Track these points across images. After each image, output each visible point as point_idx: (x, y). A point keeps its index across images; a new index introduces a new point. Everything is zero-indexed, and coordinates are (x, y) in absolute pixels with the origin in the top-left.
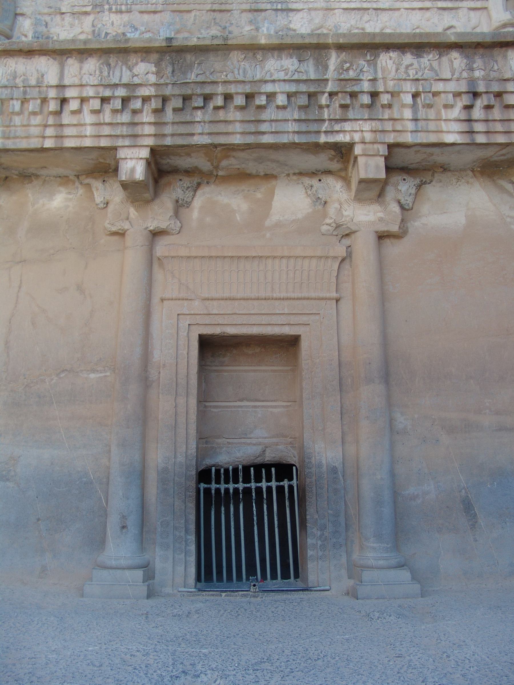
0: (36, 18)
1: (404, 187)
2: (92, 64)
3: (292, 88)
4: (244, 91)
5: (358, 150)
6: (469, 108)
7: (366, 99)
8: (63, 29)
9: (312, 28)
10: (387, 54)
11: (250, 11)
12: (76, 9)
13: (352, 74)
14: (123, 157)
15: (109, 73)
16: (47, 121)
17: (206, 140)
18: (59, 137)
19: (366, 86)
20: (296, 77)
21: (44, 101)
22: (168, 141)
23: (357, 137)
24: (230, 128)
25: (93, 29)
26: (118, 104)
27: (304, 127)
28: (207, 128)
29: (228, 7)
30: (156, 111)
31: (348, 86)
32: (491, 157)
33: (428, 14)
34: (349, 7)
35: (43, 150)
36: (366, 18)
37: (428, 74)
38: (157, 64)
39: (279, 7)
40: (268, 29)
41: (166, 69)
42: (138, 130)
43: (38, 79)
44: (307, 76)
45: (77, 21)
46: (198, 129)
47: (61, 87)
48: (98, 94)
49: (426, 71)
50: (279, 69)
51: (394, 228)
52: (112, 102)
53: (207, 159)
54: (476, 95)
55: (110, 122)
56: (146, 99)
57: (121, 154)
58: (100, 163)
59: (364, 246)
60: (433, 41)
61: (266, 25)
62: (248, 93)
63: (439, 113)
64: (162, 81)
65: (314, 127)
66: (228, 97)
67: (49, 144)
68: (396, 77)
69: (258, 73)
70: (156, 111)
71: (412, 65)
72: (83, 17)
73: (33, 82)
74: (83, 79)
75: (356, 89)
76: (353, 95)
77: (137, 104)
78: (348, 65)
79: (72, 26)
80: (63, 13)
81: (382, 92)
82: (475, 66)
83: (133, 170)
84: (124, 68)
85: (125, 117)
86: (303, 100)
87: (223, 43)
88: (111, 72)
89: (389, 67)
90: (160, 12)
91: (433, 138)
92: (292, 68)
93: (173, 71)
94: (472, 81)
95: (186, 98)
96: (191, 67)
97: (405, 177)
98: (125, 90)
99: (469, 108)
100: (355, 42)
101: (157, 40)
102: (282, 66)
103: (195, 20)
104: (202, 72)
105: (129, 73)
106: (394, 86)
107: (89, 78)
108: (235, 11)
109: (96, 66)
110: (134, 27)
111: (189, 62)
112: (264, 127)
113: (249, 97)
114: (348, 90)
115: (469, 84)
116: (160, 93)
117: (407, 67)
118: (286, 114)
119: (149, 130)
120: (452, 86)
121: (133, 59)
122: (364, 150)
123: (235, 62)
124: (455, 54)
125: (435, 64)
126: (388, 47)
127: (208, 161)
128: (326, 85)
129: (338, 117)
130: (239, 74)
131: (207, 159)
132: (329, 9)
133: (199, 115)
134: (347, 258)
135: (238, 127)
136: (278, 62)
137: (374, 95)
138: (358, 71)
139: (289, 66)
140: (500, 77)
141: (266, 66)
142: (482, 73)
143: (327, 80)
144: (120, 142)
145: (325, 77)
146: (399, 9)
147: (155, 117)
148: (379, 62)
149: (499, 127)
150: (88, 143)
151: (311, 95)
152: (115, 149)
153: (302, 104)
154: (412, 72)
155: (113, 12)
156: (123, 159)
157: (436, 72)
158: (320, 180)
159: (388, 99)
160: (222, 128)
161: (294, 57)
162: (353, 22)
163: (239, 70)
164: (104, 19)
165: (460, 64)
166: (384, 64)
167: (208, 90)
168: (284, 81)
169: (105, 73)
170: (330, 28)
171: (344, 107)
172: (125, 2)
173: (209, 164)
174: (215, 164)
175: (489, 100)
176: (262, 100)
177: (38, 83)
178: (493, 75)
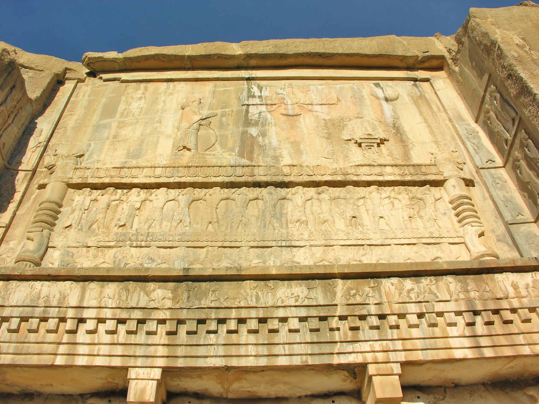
0: (65, 250)
2: (112, 288)
3: (303, 313)
4: (257, 317)
5: (372, 369)
7: (375, 321)
8: (87, 259)
9: (315, 260)
10: (390, 281)
11: (257, 247)
12: (102, 244)
13: (358, 300)
14: (133, 377)
15: (127, 297)
16: (62, 339)
17: (219, 362)
19: (373, 310)
20: (306, 303)
22: (180, 363)
23: (369, 357)
24: (242, 351)
25: (114, 260)
26: (132, 325)
27: (316, 349)
28: (221, 351)
29: (237, 244)
31: (356, 310)
32: (500, 370)
34: (346, 244)
35: (53, 367)
37: (428, 297)
38: (174, 291)
39: (284, 244)
40: (274, 262)
41: (182, 295)
42: (151, 350)
43: (59, 300)
44: (317, 301)
45: (100, 253)
46: (212, 351)
48: (115, 316)
49: (426, 294)
52: (127, 323)
53: (219, 381)
54: (476, 313)
55: (123, 342)
56: (162, 322)
58: (109, 382)
60: (428, 269)
61: (272, 259)
62: (261, 318)
63: (444, 331)
64: (178, 306)
65: (326, 348)
66: (241, 321)
67: (60, 361)
68: (400, 301)
69: (269, 300)
71: (413, 289)
72: (106, 250)
73: (55, 303)
74: (102, 301)
75: (365, 312)
76: (363, 318)
77: (152, 326)
78: (354, 291)
79: (95, 257)
80: (89, 247)
81: (389, 315)
82: (469, 288)
83: (143, 391)
84: (142, 293)
86: (314, 323)
87: (237, 274)
88: (129, 296)
89: (393, 292)
90: (176, 247)
91: (442, 355)
92: (302, 295)
93: (188, 297)
94: (469, 301)
96: (205, 294)
97: (419, 395)
98: (142, 313)
99: (471, 324)
100: (359, 271)
101: (174, 270)
102: (292, 294)
103: (207, 254)
104: (216, 299)
105: (146, 298)
106: (400, 308)
107: (108, 301)
108: (244, 248)
109: (115, 291)
110: (151, 259)
111: (204, 289)
112: (277, 350)
113: (263, 321)
114: (357, 314)
115: (467, 304)
116: (175, 317)
117: (409, 291)
118: (297, 337)
119: (162, 351)
120: (452, 306)
121: (152, 285)
122: (378, 369)
123: (248, 290)
124: (449, 279)
125: (433, 288)
126: (389, 275)
127: (220, 383)
128: (335, 310)
129: (349, 339)
130: (251, 301)
131: (219, 381)
132: (328, 246)
135: (252, 350)
136: (288, 290)
138: (364, 296)
139: (299, 294)
140: (494, 297)
141: (278, 294)
142: (477, 294)
143: (337, 305)
144: (131, 362)
145: (334, 303)
146: (390, 245)
147: (168, 339)
148: (382, 288)
149: (503, 340)
150: (99, 361)
151: (323, 319)
152: (125, 369)
153: (314, 327)
154: (413, 296)
155: (134, 247)
156: (133, 379)
157: (435, 294)
158: (333, 402)
159: (395, 321)
160: (233, 351)
161: (303, 286)
162: (351, 256)
163: (251, 297)
164: (125, 252)
165: (456, 287)
166: (387, 290)
167: (222, 315)
168: (296, 306)
169: (124, 298)
170: (330, 261)
171: (354, 329)
172: (145, 240)
173: (219, 386)
174: (226, 387)
175: (488, 317)
176: (274, 324)
177: (59, 303)
178: (487, 295)
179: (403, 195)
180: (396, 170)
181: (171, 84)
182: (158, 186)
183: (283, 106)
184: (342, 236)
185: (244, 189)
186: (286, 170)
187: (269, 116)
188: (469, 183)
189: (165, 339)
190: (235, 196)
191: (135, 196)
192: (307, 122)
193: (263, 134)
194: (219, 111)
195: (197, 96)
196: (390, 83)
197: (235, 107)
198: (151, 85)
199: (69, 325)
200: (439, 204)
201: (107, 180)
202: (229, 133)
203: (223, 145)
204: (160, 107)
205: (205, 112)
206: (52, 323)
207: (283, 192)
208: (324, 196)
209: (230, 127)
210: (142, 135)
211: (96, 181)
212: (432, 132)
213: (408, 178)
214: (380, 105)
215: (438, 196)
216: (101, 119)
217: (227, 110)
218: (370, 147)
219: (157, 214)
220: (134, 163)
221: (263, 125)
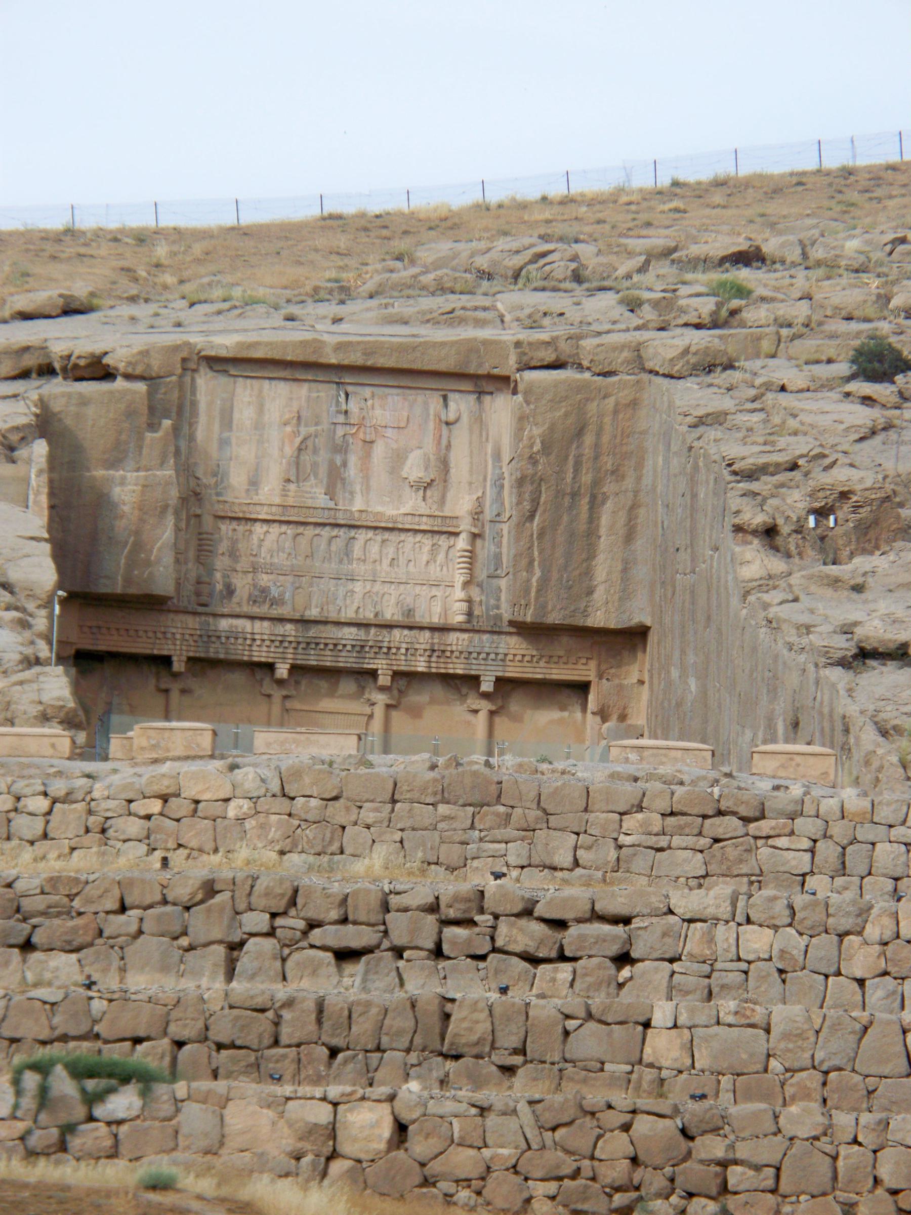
1: (402, 683)
2: (266, 624)
3: (354, 643)
5: (380, 672)
6: (430, 656)
7: (385, 650)
13: (380, 638)
18: (251, 656)
19: (386, 644)
21: (245, 639)
22: (299, 662)
26: (277, 644)
30: (295, 648)
33: (424, 587)
36: (393, 587)
47: (253, 634)
50: (350, 633)
51: (393, 702)
54: (434, 651)
56: (290, 642)
57: (278, 666)
59: (379, 711)
66: (326, 645)
67: (245, 658)
70: (295, 648)
76: (380, 648)
77: (286, 644)
85: (281, 650)
86: (358, 649)
94: (433, 644)
95: (308, 643)
99: (430, 656)
113: (335, 645)
119: (290, 656)
120: (423, 646)
126: (397, 626)
133: (312, 652)
134: (371, 716)
135: (329, 658)
137: (389, 648)
149: (442, 665)
150: (263, 660)
167: (317, 641)
176: (340, 647)
179: (427, 541)
180: (430, 521)
181: (274, 382)
182: (274, 521)
183: (362, 430)
184: (383, 574)
185: (328, 528)
186: (357, 515)
187: (351, 441)
188: (475, 536)
189: (291, 651)
190: (323, 533)
191: (259, 529)
192: (379, 450)
193: (345, 464)
194: (312, 429)
195: (295, 407)
196: (457, 396)
197: (325, 426)
198: (254, 382)
199: (248, 642)
200: (451, 550)
201: (241, 515)
202: (320, 459)
203: (316, 476)
204: (266, 417)
205: (304, 431)
206: (240, 641)
207: (353, 533)
208: (379, 538)
209: (321, 452)
210: (256, 457)
211: (233, 515)
212: (471, 472)
213: (436, 529)
214: (440, 430)
215: (452, 543)
216: (221, 433)
217: (319, 428)
218: (418, 489)
219: (275, 546)
220: (256, 499)
221: (346, 452)
